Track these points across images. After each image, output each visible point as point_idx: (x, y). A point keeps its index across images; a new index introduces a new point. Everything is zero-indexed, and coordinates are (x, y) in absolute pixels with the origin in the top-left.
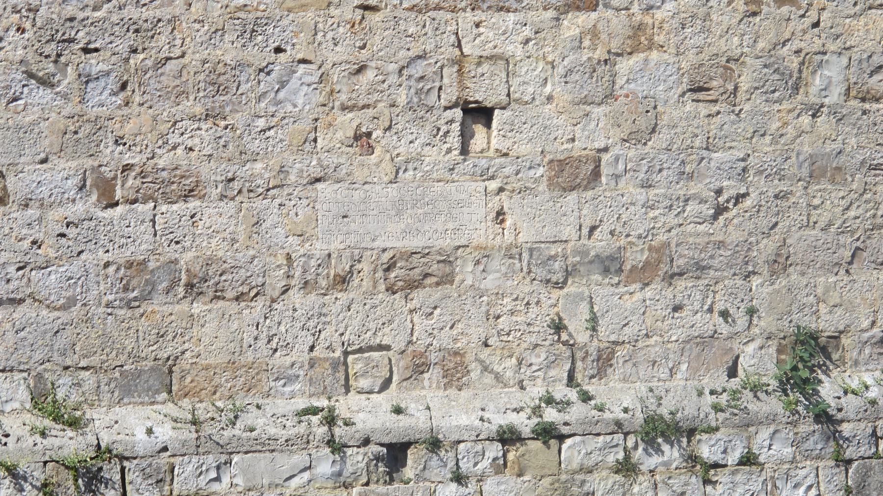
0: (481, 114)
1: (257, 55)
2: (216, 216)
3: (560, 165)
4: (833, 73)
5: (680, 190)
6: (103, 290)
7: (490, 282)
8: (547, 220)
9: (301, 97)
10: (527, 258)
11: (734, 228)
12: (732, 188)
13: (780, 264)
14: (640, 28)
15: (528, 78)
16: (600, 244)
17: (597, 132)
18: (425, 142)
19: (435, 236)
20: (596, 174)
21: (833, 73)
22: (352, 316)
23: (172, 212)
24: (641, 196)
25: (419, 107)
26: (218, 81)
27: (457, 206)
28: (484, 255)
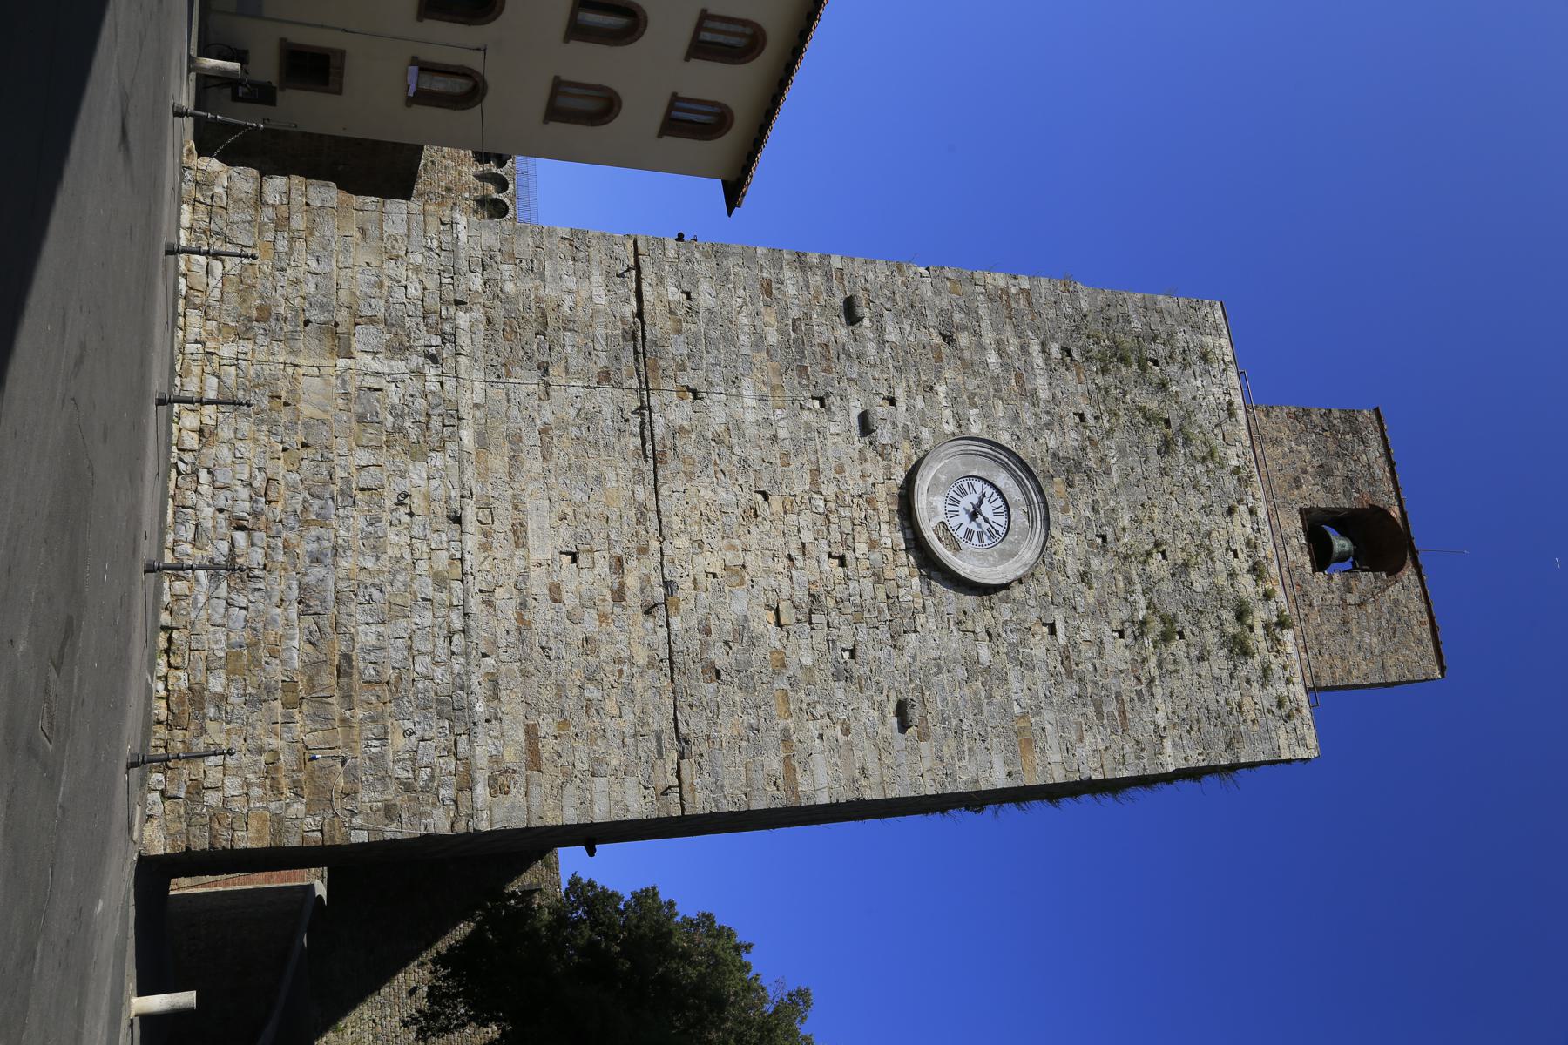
1: (590, 481)
2: (537, 466)
3: (558, 587)
4: (597, 694)
7: (516, 561)
8: (539, 583)
9: (578, 496)
10: (525, 575)
11: (537, 655)
12: (552, 654)
13: (525, 674)
15: (586, 576)
16: (531, 602)
17: (570, 601)
18: (564, 538)
19: (532, 540)
20: (555, 601)
21: (597, 694)
22: (503, 511)
25: (576, 536)
26: (581, 468)
27: (541, 549)
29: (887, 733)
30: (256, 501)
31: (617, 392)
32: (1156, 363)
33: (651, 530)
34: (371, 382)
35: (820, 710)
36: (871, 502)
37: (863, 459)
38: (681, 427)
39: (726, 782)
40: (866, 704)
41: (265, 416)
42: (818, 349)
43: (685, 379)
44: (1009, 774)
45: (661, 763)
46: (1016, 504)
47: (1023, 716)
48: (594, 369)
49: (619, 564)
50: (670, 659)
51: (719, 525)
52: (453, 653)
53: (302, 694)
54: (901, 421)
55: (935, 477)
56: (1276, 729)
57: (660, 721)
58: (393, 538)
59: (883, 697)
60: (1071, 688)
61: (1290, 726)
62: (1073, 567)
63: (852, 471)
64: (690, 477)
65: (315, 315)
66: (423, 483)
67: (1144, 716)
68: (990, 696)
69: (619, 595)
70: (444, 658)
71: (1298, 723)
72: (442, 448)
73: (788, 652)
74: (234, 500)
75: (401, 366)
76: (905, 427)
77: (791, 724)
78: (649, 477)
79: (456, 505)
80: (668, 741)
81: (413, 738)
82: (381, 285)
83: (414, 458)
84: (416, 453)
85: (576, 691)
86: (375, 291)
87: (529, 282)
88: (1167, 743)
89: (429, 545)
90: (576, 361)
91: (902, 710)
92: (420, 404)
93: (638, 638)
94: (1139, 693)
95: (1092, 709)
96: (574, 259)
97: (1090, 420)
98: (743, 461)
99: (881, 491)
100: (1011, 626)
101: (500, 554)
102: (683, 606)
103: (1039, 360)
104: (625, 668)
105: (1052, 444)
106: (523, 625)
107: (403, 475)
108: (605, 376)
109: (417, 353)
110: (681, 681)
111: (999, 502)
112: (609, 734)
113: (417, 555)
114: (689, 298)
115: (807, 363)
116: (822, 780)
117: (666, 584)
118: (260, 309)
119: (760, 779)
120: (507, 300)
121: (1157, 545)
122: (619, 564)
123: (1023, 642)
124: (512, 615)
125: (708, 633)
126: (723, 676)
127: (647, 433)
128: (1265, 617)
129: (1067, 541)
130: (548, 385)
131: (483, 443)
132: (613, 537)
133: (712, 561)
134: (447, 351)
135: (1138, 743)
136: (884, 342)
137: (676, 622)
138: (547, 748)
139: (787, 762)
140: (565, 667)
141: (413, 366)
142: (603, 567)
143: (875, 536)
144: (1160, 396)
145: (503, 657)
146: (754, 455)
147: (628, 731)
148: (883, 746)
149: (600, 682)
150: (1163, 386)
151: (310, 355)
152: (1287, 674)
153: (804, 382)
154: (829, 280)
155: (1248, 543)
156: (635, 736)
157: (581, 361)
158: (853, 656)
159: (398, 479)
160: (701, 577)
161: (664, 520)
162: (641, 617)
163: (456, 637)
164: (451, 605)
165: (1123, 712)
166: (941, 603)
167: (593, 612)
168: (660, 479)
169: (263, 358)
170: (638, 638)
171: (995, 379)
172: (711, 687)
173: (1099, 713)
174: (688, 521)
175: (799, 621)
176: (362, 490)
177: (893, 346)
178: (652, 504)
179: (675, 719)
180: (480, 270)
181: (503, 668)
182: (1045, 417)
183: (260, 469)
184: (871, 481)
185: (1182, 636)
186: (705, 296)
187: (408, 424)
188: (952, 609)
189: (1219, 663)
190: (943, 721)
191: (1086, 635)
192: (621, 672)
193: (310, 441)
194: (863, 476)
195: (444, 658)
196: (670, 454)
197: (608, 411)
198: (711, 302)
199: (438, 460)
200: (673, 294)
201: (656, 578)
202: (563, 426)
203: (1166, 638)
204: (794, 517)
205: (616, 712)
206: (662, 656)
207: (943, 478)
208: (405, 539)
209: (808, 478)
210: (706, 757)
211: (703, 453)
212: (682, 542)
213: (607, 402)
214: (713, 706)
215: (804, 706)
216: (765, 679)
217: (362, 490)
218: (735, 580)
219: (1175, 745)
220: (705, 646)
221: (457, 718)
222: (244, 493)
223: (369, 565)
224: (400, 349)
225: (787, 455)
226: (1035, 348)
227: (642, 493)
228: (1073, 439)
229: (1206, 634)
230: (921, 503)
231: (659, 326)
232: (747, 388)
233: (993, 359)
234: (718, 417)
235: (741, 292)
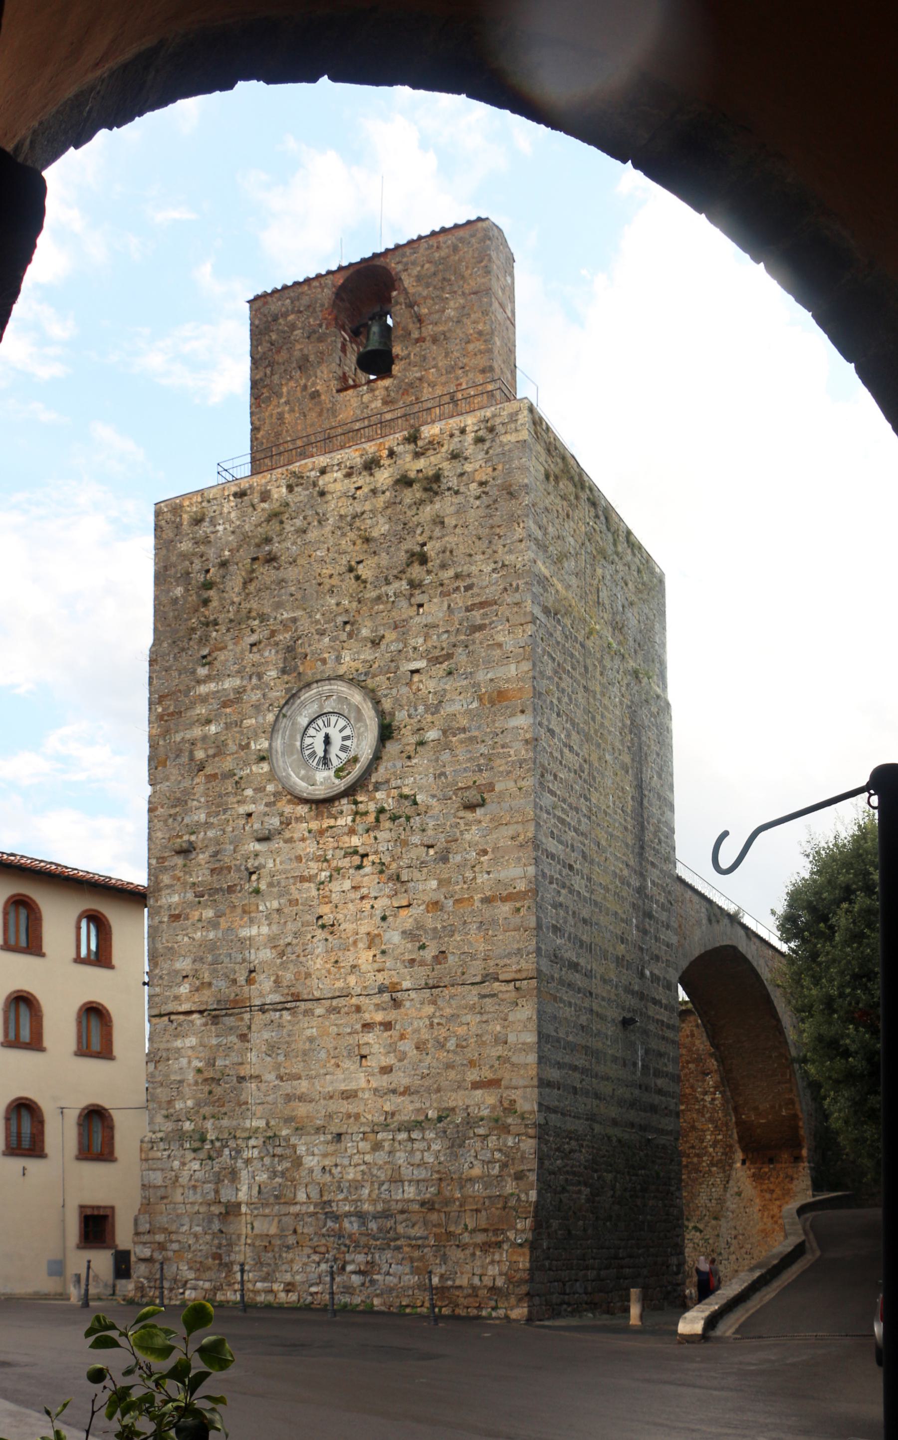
0: (363, 1057)
6: (280, 1100)
7: (366, 1096)
15: (376, 1049)
16: (391, 1087)
17: (391, 1060)
19: (353, 1086)
20: (391, 1070)
22: (333, 1106)
23: (295, 1083)
25: (349, 1056)
26: (305, 1053)
28: (363, 1090)
29: (488, 817)
31: (253, 1028)
32: (208, 571)
33: (344, 1003)
34: (255, 1191)
35: (469, 874)
36: (321, 832)
37: (290, 840)
38: (275, 982)
39: (516, 946)
40: (467, 836)
42: (215, 877)
43: (242, 979)
44: (523, 712)
45: (500, 995)
46: (321, 707)
47: (480, 699)
48: (239, 1045)
49: (367, 1026)
51: (340, 954)
54: (262, 808)
55: (302, 779)
56: (502, 445)
57: (472, 995)
58: (351, 1176)
59: (461, 821)
60: (461, 656)
61: (500, 429)
62: (367, 654)
64: (308, 975)
65: (216, 1226)
66: (316, 1158)
67: (485, 583)
68: (464, 730)
69: (387, 1026)
70: (425, 1144)
71: (498, 420)
72: (294, 1147)
73: (427, 899)
75: (244, 1174)
76: (267, 805)
77: (477, 897)
78: (309, 1005)
79: (329, 1137)
80: (486, 989)
81: (475, 1163)
82: (195, 1187)
84: (298, 1162)
85: (450, 1055)
86: (199, 1190)
87: (186, 1090)
88: (509, 559)
90: (234, 1058)
91: (470, 807)
92: (267, 1160)
93: (416, 1013)
94: (468, 588)
95: (477, 635)
96: (168, 1060)
97: (254, 638)
98: (296, 935)
99: (314, 825)
100: (412, 711)
101: (362, 1108)
102: (395, 980)
103: (212, 686)
104: (436, 1021)
105: (273, 673)
106: (407, 1091)
107: (311, 1171)
108: (244, 1037)
110: (446, 980)
111: (320, 722)
112: (479, 1032)
114: (187, 976)
115: (225, 886)
116: (517, 872)
118: (214, 1259)
119: (516, 920)
120: (198, 1104)
121: (351, 570)
122: (367, 1026)
123: (424, 700)
124: (400, 1099)
125: (412, 961)
126: (443, 949)
127: (279, 1007)
128: (408, 457)
129: (347, 659)
130: (251, 1077)
132: (349, 1030)
133: (365, 958)
134: (232, 1144)
135: (505, 589)
137: (406, 984)
138: (487, 1074)
139: (504, 900)
140: (435, 1064)
141: (243, 1166)
142: (370, 1038)
143: (346, 830)
144: (233, 568)
145: (428, 1104)
148: (497, 823)
149: (446, 1039)
150: (224, 564)
151: (242, 1227)
152: (457, 433)
154: (166, 869)
155: (348, 475)
156: (481, 1014)
157: (234, 1054)
158: (432, 846)
160: (376, 966)
161: (338, 994)
162: (403, 1010)
164: (393, 1140)
165: (482, 605)
166: (394, 773)
167: (399, 1044)
168: (311, 997)
170: (416, 1013)
171: (228, 726)
172: (451, 958)
173: (481, 628)
175: (406, 891)
176: (321, 1196)
177: (209, 815)
178: (327, 1003)
181: (435, 1105)
182: (254, 680)
184: (306, 834)
185: (424, 544)
187: (280, 1168)
188: (399, 764)
189: (445, 505)
190: (481, 771)
191: (421, 640)
192: (439, 1024)
193: (292, 1228)
194: (303, 840)
195: (425, 1144)
196: (293, 990)
197: (266, 1035)
198: (189, 960)
199: (301, 1150)
200: (184, 989)
201: (377, 1000)
202: (278, 1066)
203: (423, 559)
204: (334, 895)
205: (465, 1027)
207: (303, 772)
208: (351, 1170)
209: (306, 885)
211: (291, 966)
212: (352, 980)
213: (260, 1036)
215: (465, 886)
216: (446, 917)
217: (321, 1196)
218: (377, 940)
219: (510, 552)
220: (422, 963)
221: (464, 1135)
223: (367, 1191)
224: (234, 1175)
225: (290, 901)
226: (203, 689)
227: (319, 1011)
228: (270, 654)
229: (422, 520)
230: (320, 792)
231: (207, 998)
232: (244, 933)
233: (213, 729)
234: (266, 954)
235: (179, 938)
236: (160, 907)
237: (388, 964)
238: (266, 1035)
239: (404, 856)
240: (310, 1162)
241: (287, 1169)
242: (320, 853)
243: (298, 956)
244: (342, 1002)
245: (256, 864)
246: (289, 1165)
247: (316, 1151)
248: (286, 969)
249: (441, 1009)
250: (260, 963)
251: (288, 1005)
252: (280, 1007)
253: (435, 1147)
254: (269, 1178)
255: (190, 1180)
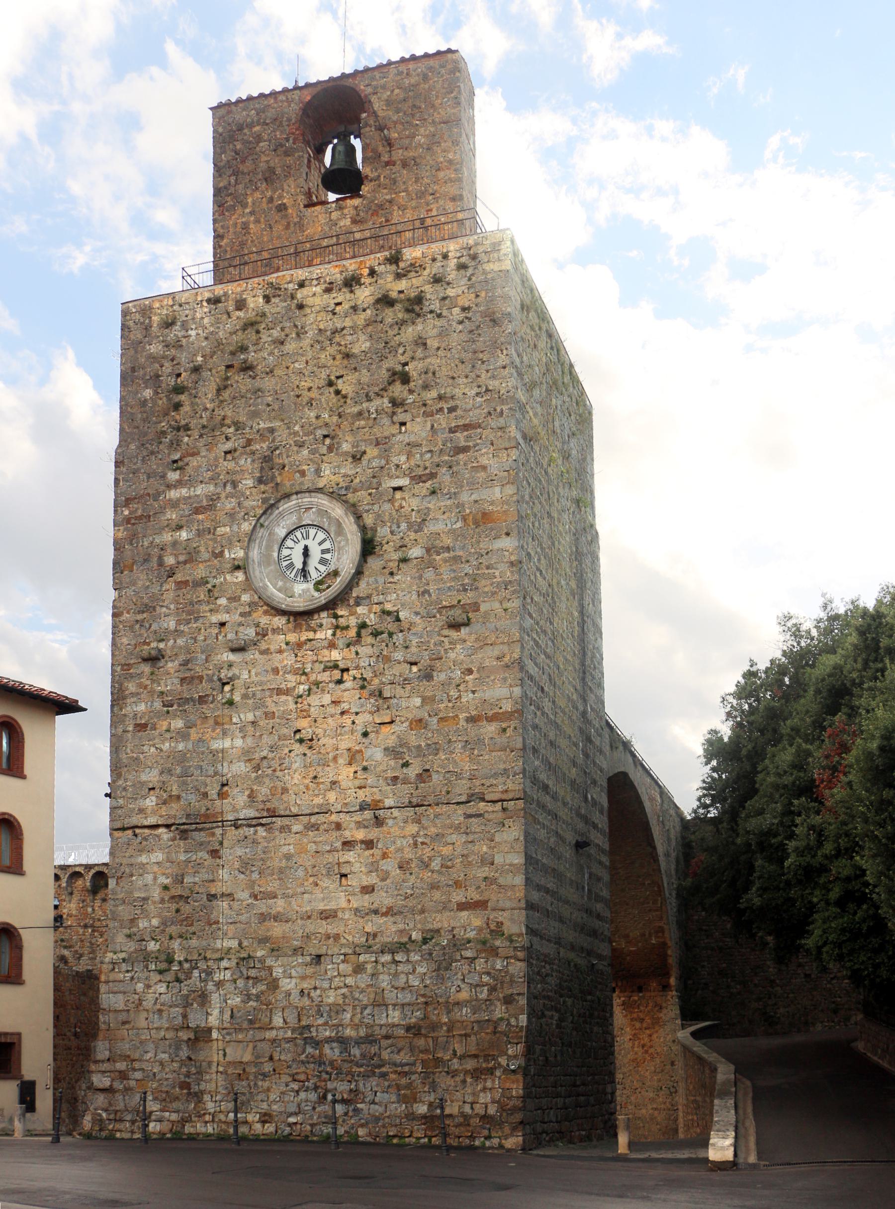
3: (363, 888)
5: (396, 893)
7: (346, 917)
10: (357, 910)
14: (385, 853)
17: (373, 879)
19: (332, 906)
20: (373, 890)
24: (384, 895)
25: (328, 874)
30: (308, 1087)
36: (300, 645)
38: (249, 796)
41: (252, 1084)
42: (185, 687)
43: (213, 793)
48: (209, 861)
49: (348, 844)
50: (414, 807)
52: (408, 960)
53: (431, 1057)
57: (458, 815)
58: (331, 1000)
63: (277, 660)
64: (285, 790)
66: (294, 981)
69: (369, 844)
70: (410, 967)
72: (270, 969)
73: (410, 716)
74: (307, 1101)
77: (462, 716)
78: (286, 821)
79: (308, 959)
82: (160, 1011)
83: (277, 987)
84: (274, 985)
86: (165, 1014)
89: (335, 977)
92: (241, 983)
93: (399, 832)
96: (132, 876)
99: (292, 637)
104: (420, 840)
108: (215, 854)
109: (205, 986)
110: (431, 799)
112: (465, 852)
113: (342, 984)
114: (154, 789)
115: (196, 696)
117: (362, 808)
122: (348, 844)
125: (395, 778)
126: (428, 767)
127: (254, 822)
130: (223, 895)
131: (263, 941)
132: (328, 848)
133: (345, 774)
134: (202, 965)
136: (176, 631)
137: (388, 802)
141: (214, 988)
142: (350, 856)
145: (411, 925)
146: (267, 740)
147: (464, 838)
153: (211, 698)
154: (132, 676)
156: (467, 834)
158: (415, 664)
159: (291, 998)
160: (357, 783)
161: (316, 810)
163: (396, 958)
164: (376, 962)
169: (214, 1085)
170: (399, 832)
172: (435, 776)
174: (316, 792)
176: (299, 1020)
177: (179, 622)
178: (305, 819)
179: (458, 803)
180: (144, 943)
181: (419, 926)
183: (287, 1086)
184: (284, 646)
186: (151, 776)
187: (254, 991)
192: (423, 843)
193: (267, 1055)
194: (280, 652)
195: (410, 967)
197: (239, 852)
198: (155, 772)
199: (278, 972)
201: (358, 817)
204: (312, 709)
206: (412, 813)
208: (332, 993)
210: (484, 781)
211: (267, 780)
212: (332, 796)
213: (233, 853)
214: (447, 776)
215: (450, 705)
217: (299, 1020)
218: (358, 756)
222: (303, 1095)
223: (349, 1016)
224: (203, 998)
225: (266, 714)
231: (175, 811)
232: (216, 745)
234: (240, 768)
236: (125, 715)
237: (369, 781)
238: (239, 852)
239: (387, 672)
240: (287, 984)
241: (262, 993)
242: (299, 665)
243: (274, 771)
244: (321, 818)
245: (230, 675)
246: (264, 988)
247: (294, 973)
248: (261, 784)
249: (426, 828)
250: (233, 777)
251: (264, 821)
252: (254, 823)
253: (420, 970)
254: (242, 1001)
255: (155, 1003)
